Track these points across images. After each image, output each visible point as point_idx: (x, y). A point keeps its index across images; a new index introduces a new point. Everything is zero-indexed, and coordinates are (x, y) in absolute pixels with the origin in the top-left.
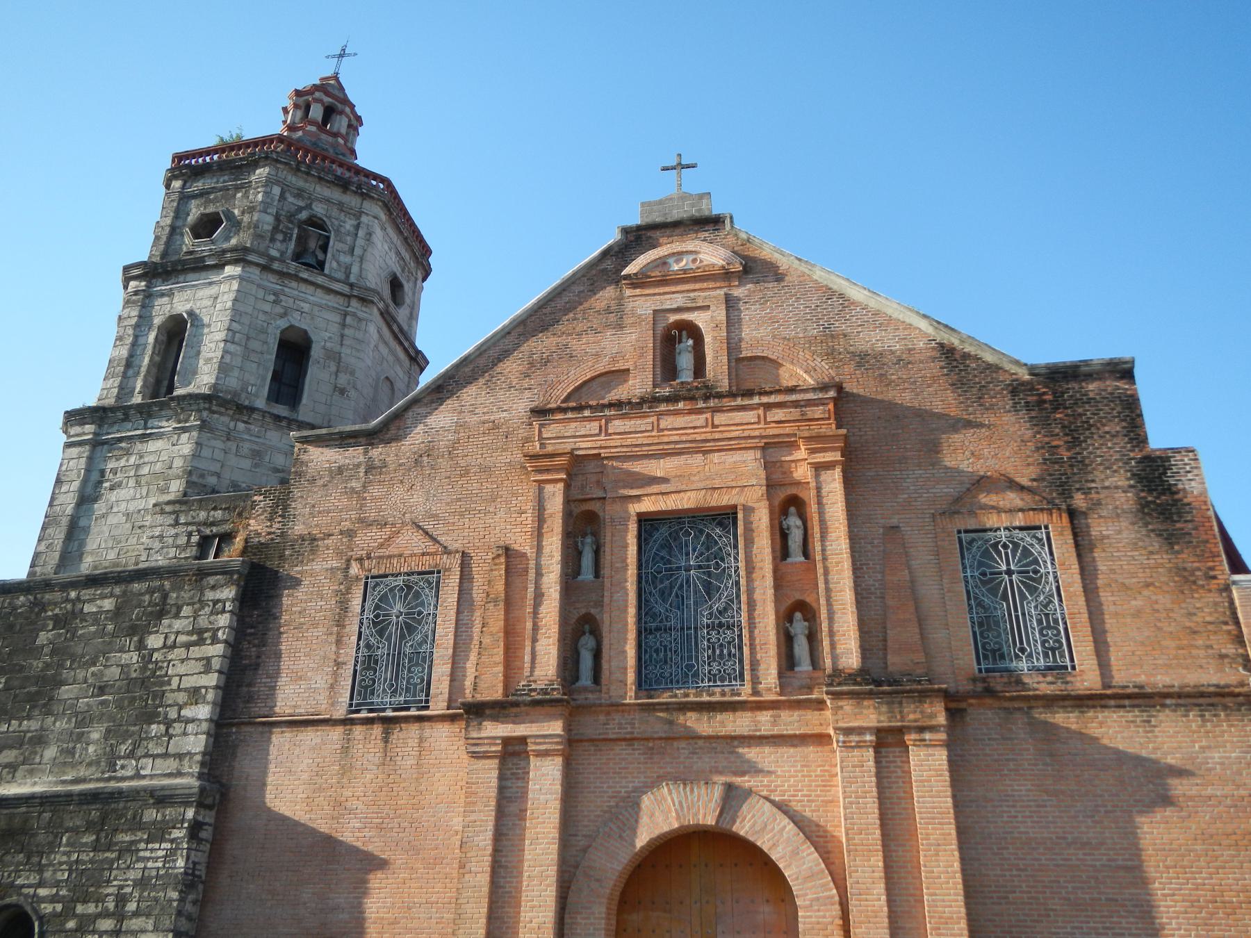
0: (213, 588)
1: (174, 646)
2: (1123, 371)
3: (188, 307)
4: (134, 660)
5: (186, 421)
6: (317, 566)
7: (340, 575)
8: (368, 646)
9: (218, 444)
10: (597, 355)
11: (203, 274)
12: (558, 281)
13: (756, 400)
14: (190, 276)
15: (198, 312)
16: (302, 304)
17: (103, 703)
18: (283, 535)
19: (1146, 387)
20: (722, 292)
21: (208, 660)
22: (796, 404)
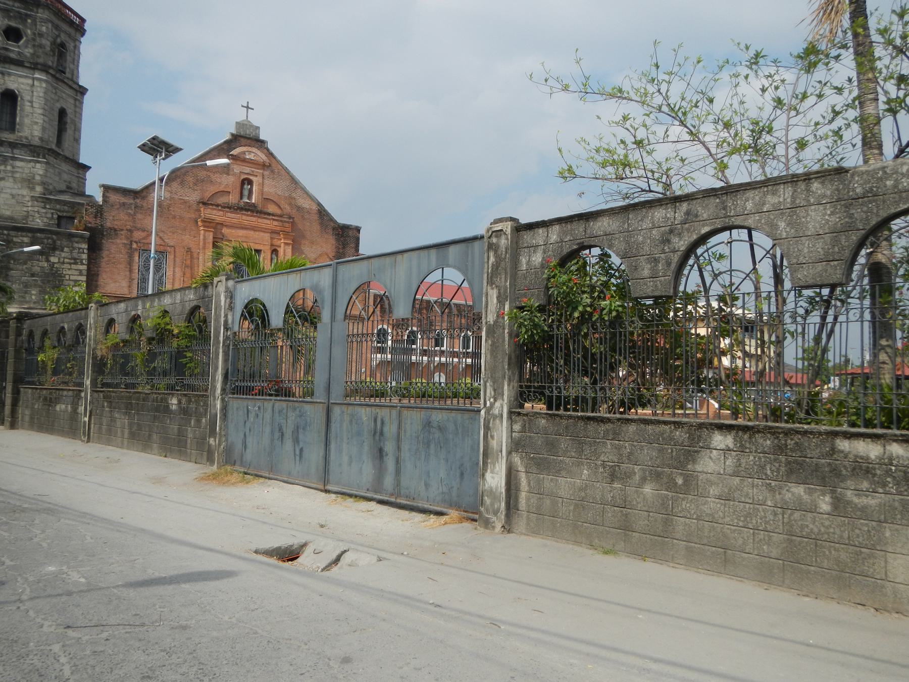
0: (77, 243)
1: (63, 263)
2: (358, 230)
3: (16, 85)
4: (46, 265)
5: (39, 158)
6: (118, 241)
7: (128, 246)
8: (143, 275)
9: (51, 170)
10: (220, 183)
11: (20, 69)
12: (208, 149)
13: (271, 217)
14: (12, 67)
15: (21, 91)
16: (64, 95)
17: (34, 280)
18: (102, 225)
19: (362, 235)
20: (261, 171)
21: (81, 271)
22: (281, 221)
